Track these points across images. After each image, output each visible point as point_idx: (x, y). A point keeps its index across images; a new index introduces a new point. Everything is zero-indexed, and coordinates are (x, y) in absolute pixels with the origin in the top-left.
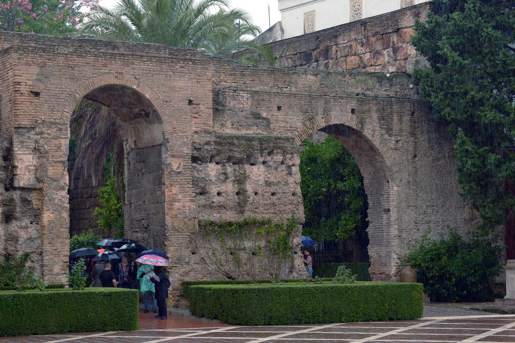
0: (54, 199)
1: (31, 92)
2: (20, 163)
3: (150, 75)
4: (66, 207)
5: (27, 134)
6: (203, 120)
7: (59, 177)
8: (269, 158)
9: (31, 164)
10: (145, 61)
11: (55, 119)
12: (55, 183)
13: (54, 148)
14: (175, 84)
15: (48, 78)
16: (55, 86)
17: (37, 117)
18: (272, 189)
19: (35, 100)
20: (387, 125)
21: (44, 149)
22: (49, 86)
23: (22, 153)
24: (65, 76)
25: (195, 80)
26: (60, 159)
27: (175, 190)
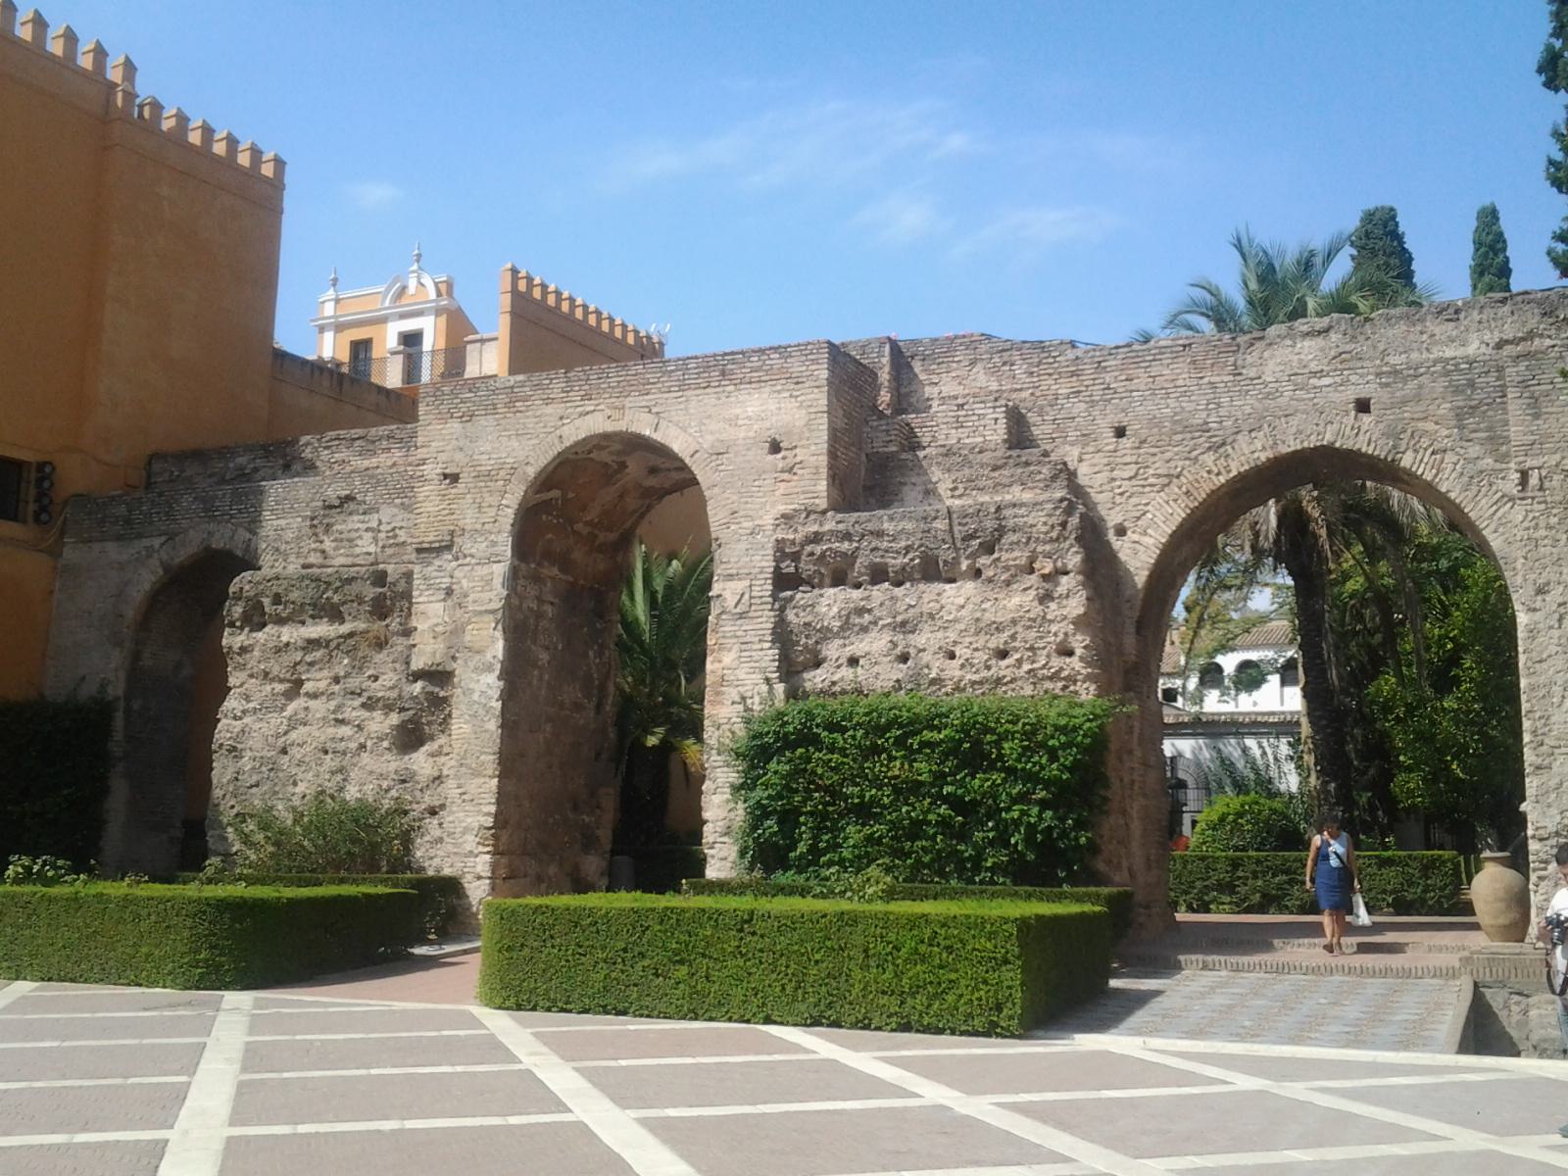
0: (472, 691)
1: (446, 476)
4: (495, 709)
5: (437, 563)
6: (802, 483)
8: (983, 561)
9: (440, 620)
10: (673, 371)
11: (484, 524)
14: (738, 411)
18: (998, 641)
20: (1489, 429)
21: (461, 588)
22: (475, 457)
25: (787, 394)
27: (728, 658)
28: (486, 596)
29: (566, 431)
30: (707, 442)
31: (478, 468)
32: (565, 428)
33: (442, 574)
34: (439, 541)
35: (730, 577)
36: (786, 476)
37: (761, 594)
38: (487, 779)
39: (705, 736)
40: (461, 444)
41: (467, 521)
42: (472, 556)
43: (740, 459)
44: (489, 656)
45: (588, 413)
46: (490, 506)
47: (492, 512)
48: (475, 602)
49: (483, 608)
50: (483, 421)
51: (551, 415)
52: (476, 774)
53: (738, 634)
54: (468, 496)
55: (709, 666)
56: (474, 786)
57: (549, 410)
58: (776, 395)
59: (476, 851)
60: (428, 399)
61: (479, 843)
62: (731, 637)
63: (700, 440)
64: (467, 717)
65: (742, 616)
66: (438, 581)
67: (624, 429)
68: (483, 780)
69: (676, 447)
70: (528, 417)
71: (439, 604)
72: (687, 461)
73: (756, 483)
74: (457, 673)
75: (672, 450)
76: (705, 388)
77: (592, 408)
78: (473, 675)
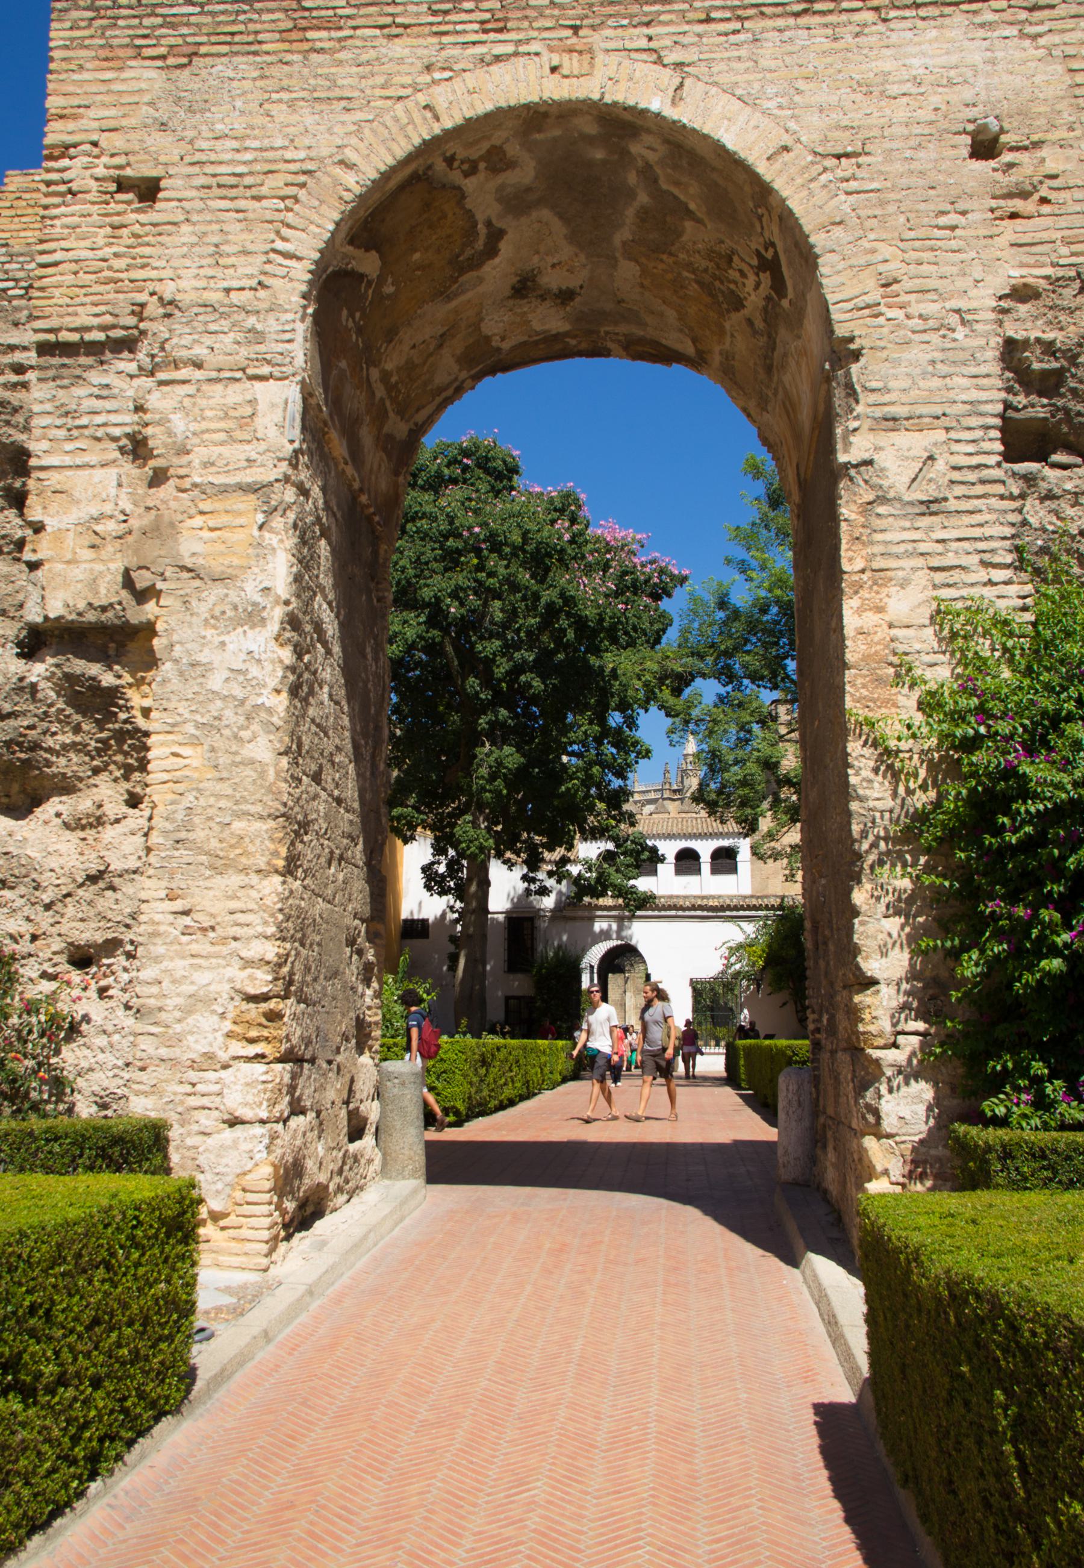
0: (207, 669)
1: (122, 185)
2: (53, 508)
3: (742, 37)
4: (270, 711)
5: (95, 377)
6: (1063, 222)
7: (236, 562)
9: (108, 508)
11: (228, 291)
12: (219, 590)
13: (222, 425)
14: (888, 66)
15: (203, 111)
16: (235, 144)
17: (141, 291)
19: (135, 217)
21: (170, 433)
22: (205, 145)
23: (68, 460)
24: (285, 96)
25: (1013, 31)
26: (248, 477)
28: (237, 453)
29: (441, 96)
30: (811, 129)
31: (210, 169)
32: (436, 90)
33: (108, 405)
34: (103, 328)
35: (892, 422)
36: (1017, 205)
37: (975, 460)
38: (254, 879)
39: (853, 780)
40: (163, 115)
41: (182, 284)
42: (198, 365)
43: (898, 167)
44: (251, 590)
45: (498, 59)
46: (245, 253)
47: (249, 268)
48: (207, 464)
49: (231, 480)
50: (221, 68)
51: (401, 61)
52: (219, 865)
53: (923, 547)
54: (185, 228)
55: (851, 620)
56: (212, 896)
57: (399, 48)
58: (981, 33)
59: (223, 1056)
60: (75, 14)
61: (229, 1035)
62: (909, 555)
63: (792, 125)
64: (190, 728)
65: (930, 507)
66: (99, 419)
67: (596, 96)
68: (235, 880)
69: (730, 141)
70: (340, 63)
71: (99, 474)
72: (762, 169)
73: (943, 221)
74: (160, 627)
75: (720, 149)
76: (797, 15)
77: (510, 49)
78: (209, 633)
